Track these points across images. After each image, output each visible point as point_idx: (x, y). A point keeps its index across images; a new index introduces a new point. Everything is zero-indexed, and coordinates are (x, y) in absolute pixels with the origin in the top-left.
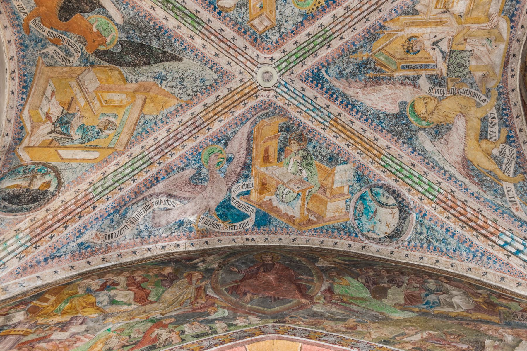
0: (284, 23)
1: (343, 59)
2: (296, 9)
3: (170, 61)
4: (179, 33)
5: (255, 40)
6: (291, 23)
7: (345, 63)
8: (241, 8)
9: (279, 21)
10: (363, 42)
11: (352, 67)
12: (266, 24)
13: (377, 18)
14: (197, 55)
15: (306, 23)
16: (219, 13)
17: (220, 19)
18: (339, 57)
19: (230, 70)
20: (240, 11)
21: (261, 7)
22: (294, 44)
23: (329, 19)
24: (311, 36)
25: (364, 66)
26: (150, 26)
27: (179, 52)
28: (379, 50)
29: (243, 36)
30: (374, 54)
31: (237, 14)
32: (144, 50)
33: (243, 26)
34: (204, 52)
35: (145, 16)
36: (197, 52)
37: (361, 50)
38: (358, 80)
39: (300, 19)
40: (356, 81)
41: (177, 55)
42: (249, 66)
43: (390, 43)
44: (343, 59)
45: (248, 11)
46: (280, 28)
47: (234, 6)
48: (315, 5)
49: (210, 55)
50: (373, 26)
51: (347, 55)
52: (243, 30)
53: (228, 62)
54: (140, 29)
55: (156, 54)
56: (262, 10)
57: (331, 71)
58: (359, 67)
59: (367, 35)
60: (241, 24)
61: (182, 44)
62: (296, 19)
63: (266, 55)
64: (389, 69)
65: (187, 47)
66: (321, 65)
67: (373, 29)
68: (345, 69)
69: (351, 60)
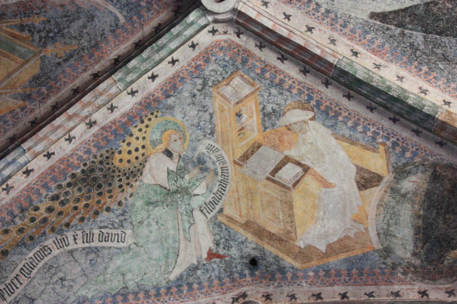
0: (198, 93)
1: (90, 42)
2: (179, 117)
3: (390, 12)
4: (376, 58)
5: (244, 62)
6: (186, 94)
7: (85, 35)
8: (274, 111)
9: (206, 95)
10: (57, 73)
11: (71, 30)
12: (229, 89)
13: (37, 111)
14: (344, 26)
15: (159, 94)
16: (310, 98)
17: (308, 89)
18: (96, 44)
19: (284, 6)
20: (274, 106)
21: (239, 115)
22: (177, 61)
23: (120, 105)
24: (149, 74)
25: (51, 35)
26: (427, 64)
27: (376, 27)
28: (27, 62)
29: (266, 66)
30: (35, 55)
31: (280, 99)
32: (438, 26)
33: (268, 82)
34: (331, 33)
35: (435, 78)
36: (345, 30)
37: (60, 60)
38: (59, 8)
39: (170, 101)
40: (62, 6)
41: (378, 23)
42: (251, 10)
43: (9, 75)
44: (90, 42)
45: (261, 107)
46: (204, 84)
47: (285, 113)
48: (147, 126)
49: (323, 28)
50: (43, 98)
51: (83, 49)
52: (268, 75)
53: (289, 20)
54: (445, 58)
55: (416, 22)
56: (237, 110)
57: (108, 20)
58: (59, 31)
59: (52, 83)
60: (272, 84)
61: (372, 41)
62: (178, 101)
63: (225, 37)
64: (6, 32)
65: (362, 38)
66: (126, 30)
67: (43, 93)
68: (85, 26)
69: (74, 42)
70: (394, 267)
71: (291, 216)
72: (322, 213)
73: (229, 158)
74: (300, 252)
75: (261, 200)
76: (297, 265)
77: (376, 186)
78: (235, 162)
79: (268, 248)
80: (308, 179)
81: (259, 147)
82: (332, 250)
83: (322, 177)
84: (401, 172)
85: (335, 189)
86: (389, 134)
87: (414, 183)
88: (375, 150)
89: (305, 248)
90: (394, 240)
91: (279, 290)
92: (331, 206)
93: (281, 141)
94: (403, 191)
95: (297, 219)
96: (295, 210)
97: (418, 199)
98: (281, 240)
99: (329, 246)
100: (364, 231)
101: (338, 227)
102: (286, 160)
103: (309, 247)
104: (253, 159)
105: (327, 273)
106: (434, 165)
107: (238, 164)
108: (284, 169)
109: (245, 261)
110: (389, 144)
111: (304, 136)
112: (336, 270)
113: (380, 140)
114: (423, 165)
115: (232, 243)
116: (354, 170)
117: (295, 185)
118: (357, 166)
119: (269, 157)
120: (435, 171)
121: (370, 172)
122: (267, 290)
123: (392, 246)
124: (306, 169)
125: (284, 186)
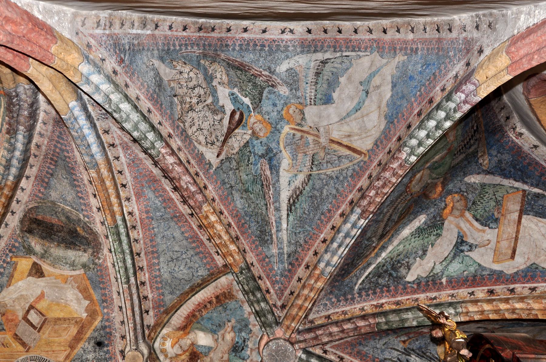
70: (95, 264)
71: (65, 319)
72: (62, 301)
73: (23, 355)
74: (90, 316)
75: (54, 337)
76: (99, 319)
77: (40, 266)
78: (27, 351)
79: (88, 335)
80: (39, 306)
81: (16, 335)
82: (88, 297)
83: (37, 298)
84: (29, 251)
85: (45, 291)
86: (4, 254)
87: (36, 244)
88: (16, 264)
89: (87, 313)
90: (77, 262)
91: (118, 330)
92: (57, 294)
93: (12, 320)
94: (43, 252)
95: (66, 316)
96: (61, 317)
97: (47, 244)
98: (82, 327)
99: (86, 298)
100: (72, 278)
101: (72, 292)
102: (25, 318)
103: (86, 310)
104: (25, 339)
105: (103, 301)
106: (22, 231)
107: (28, 349)
108: (32, 321)
109: (97, 350)
110: (11, 254)
111: (8, 305)
112: (102, 296)
113: (9, 259)
114: (23, 237)
115: (84, 358)
116: (30, 278)
117: (43, 315)
118: (28, 276)
119: (23, 329)
120: (26, 231)
121: (31, 270)
122: (118, 337)
123: (81, 263)
124: (31, 307)
125: (44, 322)
